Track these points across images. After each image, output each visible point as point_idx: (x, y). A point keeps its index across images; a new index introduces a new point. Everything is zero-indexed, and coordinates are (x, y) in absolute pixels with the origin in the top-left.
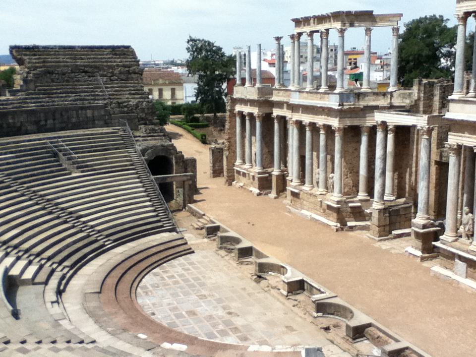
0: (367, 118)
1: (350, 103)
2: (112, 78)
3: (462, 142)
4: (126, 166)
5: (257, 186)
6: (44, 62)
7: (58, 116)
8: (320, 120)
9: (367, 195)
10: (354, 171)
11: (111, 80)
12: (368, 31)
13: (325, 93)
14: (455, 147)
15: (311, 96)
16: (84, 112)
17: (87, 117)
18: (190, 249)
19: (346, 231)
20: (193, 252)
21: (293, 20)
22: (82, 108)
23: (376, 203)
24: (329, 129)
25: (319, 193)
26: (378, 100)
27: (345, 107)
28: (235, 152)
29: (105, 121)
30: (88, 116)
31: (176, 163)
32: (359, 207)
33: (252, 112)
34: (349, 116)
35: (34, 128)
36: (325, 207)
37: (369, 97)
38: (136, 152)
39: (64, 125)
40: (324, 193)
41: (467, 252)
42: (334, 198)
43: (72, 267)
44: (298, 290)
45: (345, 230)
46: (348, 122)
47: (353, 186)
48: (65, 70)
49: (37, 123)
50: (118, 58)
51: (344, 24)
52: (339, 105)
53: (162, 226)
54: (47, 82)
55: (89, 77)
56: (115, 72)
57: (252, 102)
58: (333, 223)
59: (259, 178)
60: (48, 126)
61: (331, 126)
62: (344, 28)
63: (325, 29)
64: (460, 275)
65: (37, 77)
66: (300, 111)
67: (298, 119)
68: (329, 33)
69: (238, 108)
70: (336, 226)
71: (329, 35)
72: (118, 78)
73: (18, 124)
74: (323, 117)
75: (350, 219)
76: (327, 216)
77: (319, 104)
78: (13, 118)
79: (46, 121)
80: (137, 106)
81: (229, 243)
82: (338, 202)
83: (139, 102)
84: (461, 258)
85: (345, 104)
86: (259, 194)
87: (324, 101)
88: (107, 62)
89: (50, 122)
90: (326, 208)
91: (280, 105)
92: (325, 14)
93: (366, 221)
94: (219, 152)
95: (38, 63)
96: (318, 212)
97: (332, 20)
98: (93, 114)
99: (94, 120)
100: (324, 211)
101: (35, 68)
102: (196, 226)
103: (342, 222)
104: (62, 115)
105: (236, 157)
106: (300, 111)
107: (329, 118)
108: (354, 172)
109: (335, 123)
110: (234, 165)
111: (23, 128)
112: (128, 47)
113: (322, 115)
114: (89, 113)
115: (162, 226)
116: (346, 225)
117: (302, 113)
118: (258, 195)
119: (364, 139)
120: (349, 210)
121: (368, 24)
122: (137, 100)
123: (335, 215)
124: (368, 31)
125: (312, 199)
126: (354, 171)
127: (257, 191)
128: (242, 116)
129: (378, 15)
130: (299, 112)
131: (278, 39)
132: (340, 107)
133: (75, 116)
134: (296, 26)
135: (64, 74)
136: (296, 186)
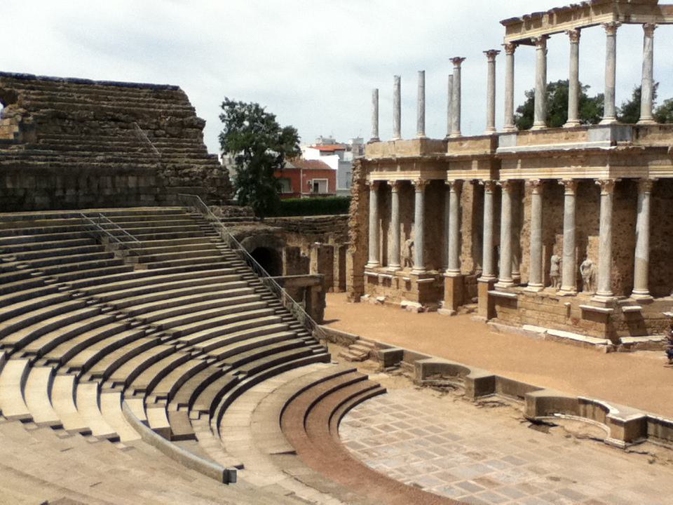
0: (650, 167)
1: (625, 142)
2: (157, 132)
4: (215, 260)
5: (416, 296)
6: (49, 100)
7: (83, 183)
9: (647, 292)
10: (620, 255)
11: (156, 136)
12: (649, 31)
13: (576, 129)
15: (544, 138)
16: (124, 179)
17: (128, 188)
18: (379, 386)
19: (621, 351)
20: (384, 391)
21: (504, 23)
22: (121, 173)
24: (586, 189)
25: (562, 293)
26: (666, 138)
27: (620, 148)
28: (366, 248)
29: (156, 196)
31: (288, 259)
32: (637, 312)
33: (407, 179)
34: (623, 162)
35: (45, 200)
36: (577, 313)
37: (653, 134)
38: (223, 241)
39: (91, 199)
40: (573, 292)
42: (600, 297)
43: (211, 412)
44: (639, 437)
45: (618, 349)
46: (623, 173)
47: (619, 280)
48: (85, 114)
49: (50, 192)
50: (164, 103)
51: (617, 17)
52: (612, 145)
53: (310, 353)
54: (56, 132)
55: (122, 128)
56: (162, 123)
57: (406, 164)
58: (600, 341)
59: (420, 284)
60: (67, 200)
61: (592, 179)
62: (617, 22)
63: (576, 29)
65: (40, 121)
66: (519, 165)
68: (580, 36)
69: (374, 177)
70: (606, 344)
71: (580, 38)
72: (167, 133)
73: (21, 193)
74: (573, 167)
75: (624, 332)
76: (585, 330)
77: (565, 147)
78: (14, 182)
79: (65, 192)
81: (438, 376)
82: (608, 304)
83: (207, 168)
85: (618, 142)
86: (421, 311)
87: (580, 141)
88: (148, 107)
89: (70, 192)
90: (580, 316)
91: (463, 163)
92: (569, 6)
93: (647, 335)
94: (328, 252)
95: (41, 100)
97: (592, 12)
98: (137, 183)
99: (139, 194)
100: (576, 321)
101: (37, 108)
102: (352, 357)
103: (612, 335)
104: (88, 181)
105: (368, 255)
106: (519, 165)
107: (587, 168)
108: (620, 257)
109: (601, 174)
110: (364, 268)
111: (28, 200)
112: (176, 88)
113: (569, 166)
114: (132, 181)
115: (310, 353)
116: (620, 342)
117: (523, 167)
118: (419, 312)
120: (623, 316)
121: (649, 19)
122: (203, 166)
123: (603, 326)
124: (649, 31)
125: (547, 305)
126: (620, 255)
127: (418, 305)
128: (383, 188)
129: (665, 6)
130: (515, 167)
131: (458, 61)
132: (613, 147)
133: (109, 185)
134: (508, 32)
135: (82, 121)
136: (508, 287)
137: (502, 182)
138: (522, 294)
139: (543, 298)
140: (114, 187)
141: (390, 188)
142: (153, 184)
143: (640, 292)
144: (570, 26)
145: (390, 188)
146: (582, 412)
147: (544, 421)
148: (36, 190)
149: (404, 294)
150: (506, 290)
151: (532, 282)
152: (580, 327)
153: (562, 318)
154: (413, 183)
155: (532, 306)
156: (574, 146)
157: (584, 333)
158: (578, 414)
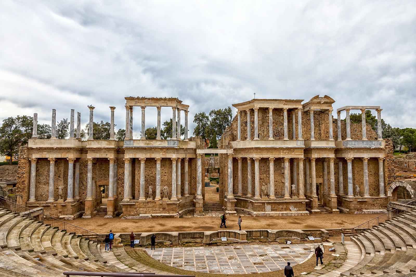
3: (263, 157)
8: (158, 156)
14: (260, 159)
21: (126, 98)
23: (200, 196)
33: (65, 157)
41: (270, 200)
64: (268, 211)
67: (131, 157)
69: (35, 156)
76: (168, 211)
84: (269, 203)
96: (157, 212)
100: (164, 209)
119: (179, 165)
125: (150, 205)
127: (73, 216)
137: (126, 159)
138: (137, 202)
139: (148, 202)
141: (49, 161)
143: (180, 196)
144: (157, 105)
145: (49, 161)
146: (219, 236)
147: (212, 242)
149: (60, 212)
150: (128, 202)
151: (142, 197)
152: (166, 211)
153: (157, 209)
154: (68, 159)
155: (143, 206)
156: (162, 146)
157: (168, 212)
158: (218, 237)
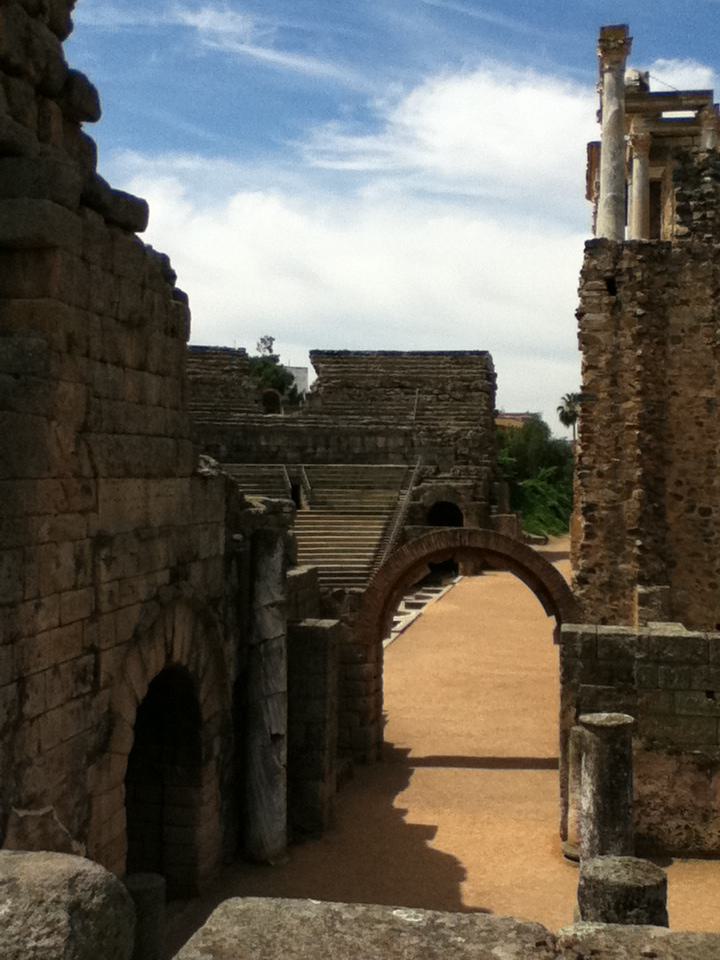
2: (440, 397)
11: (439, 400)
16: (373, 439)
17: (377, 447)
22: (371, 434)
30: (380, 446)
48: (372, 383)
49: (301, 449)
54: (342, 399)
55: (407, 394)
72: (451, 397)
73: (274, 449)
78: (267, 440)
79: (315, 449)
80: (457, 436)
98: (386, 442)
104: (339, 441)
114: (381, 441)
135: (369, 389)
140: (363, 445)
142: (401, 444)
148: (288, 447)
